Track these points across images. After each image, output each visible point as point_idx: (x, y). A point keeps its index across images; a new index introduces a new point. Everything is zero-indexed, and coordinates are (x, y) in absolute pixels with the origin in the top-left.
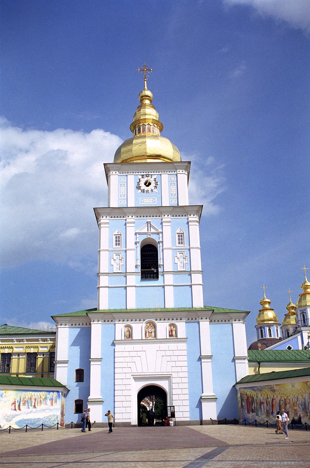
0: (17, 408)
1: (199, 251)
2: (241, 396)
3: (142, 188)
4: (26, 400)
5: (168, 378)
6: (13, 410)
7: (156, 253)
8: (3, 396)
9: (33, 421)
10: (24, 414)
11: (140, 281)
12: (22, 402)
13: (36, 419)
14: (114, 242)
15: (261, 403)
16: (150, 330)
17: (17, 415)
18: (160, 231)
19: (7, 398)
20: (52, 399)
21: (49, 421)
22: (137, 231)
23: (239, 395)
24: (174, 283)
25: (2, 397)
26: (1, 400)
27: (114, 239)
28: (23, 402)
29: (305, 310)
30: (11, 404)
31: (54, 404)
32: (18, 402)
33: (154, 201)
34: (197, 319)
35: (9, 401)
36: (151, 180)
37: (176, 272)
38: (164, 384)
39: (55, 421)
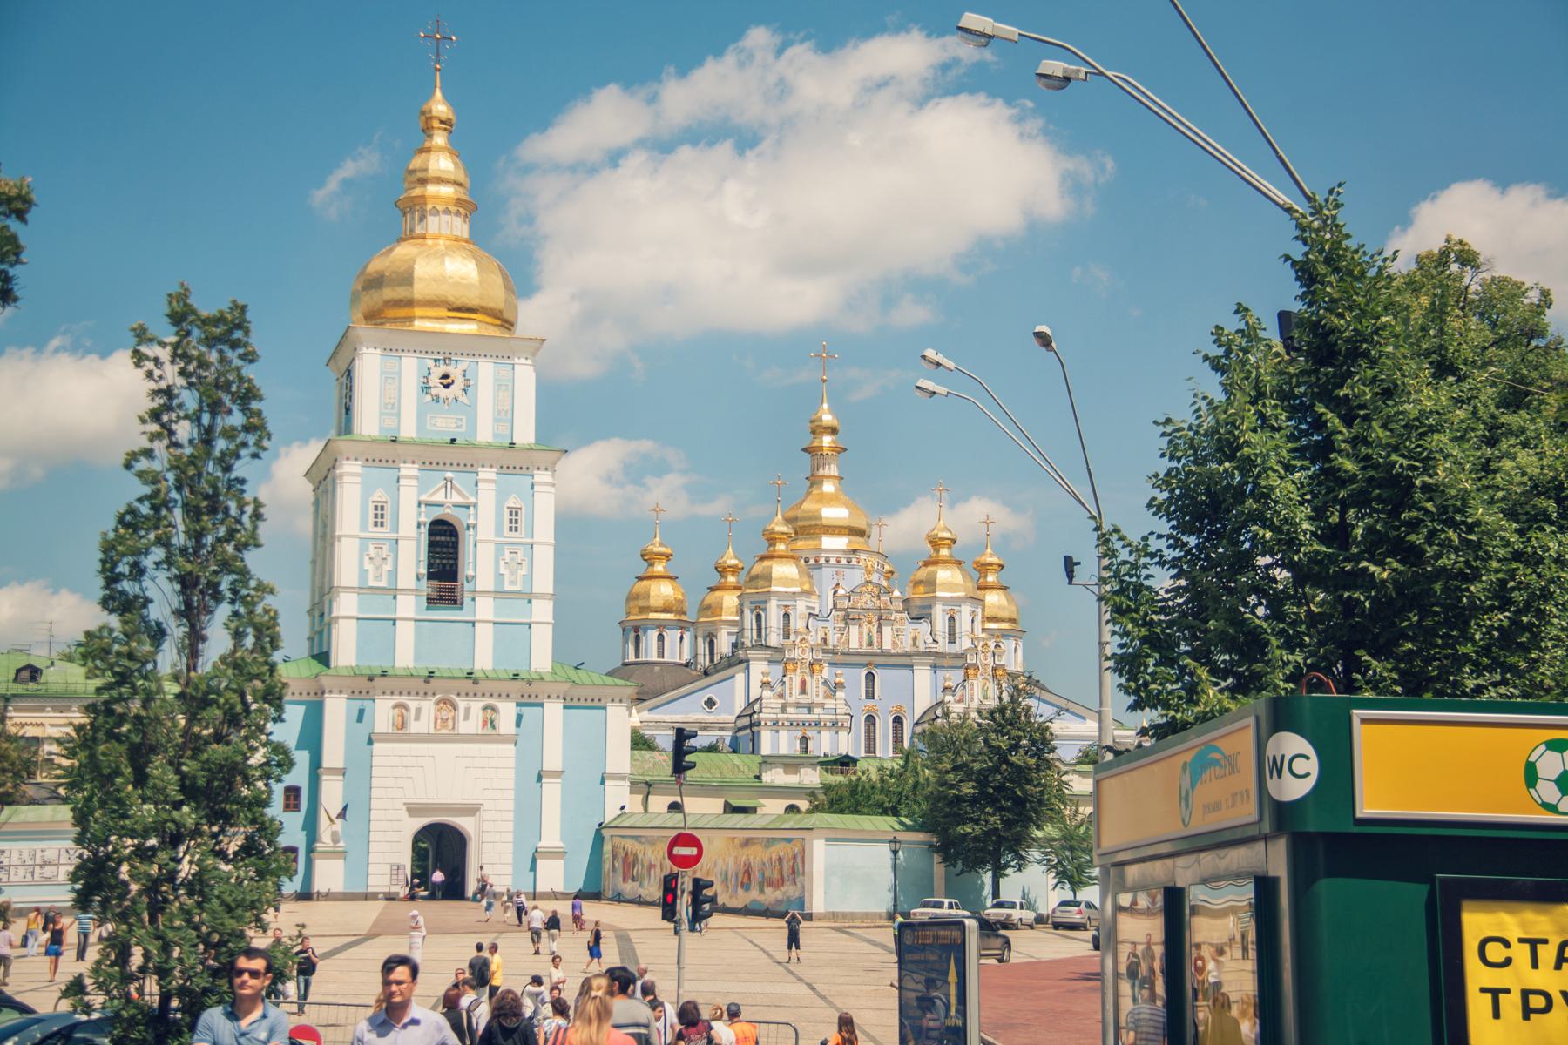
1: (552, 549)
2: (613, 851)
3: (434, 391)
5: (472, 811)
7: (453, 539)
11: (428, 609)
14: (371, 520)
15: (651, 866)
16: (444, 715)
18: (472, 500)
22: (424, 498)
23: (607, 848)
24: (496, 614)
27: (371, 512)
29: (765, 602)
33: (459, 423)
34: (540, 697)
36: (455, 372)
37: (499, 594)
38: (464, 823)
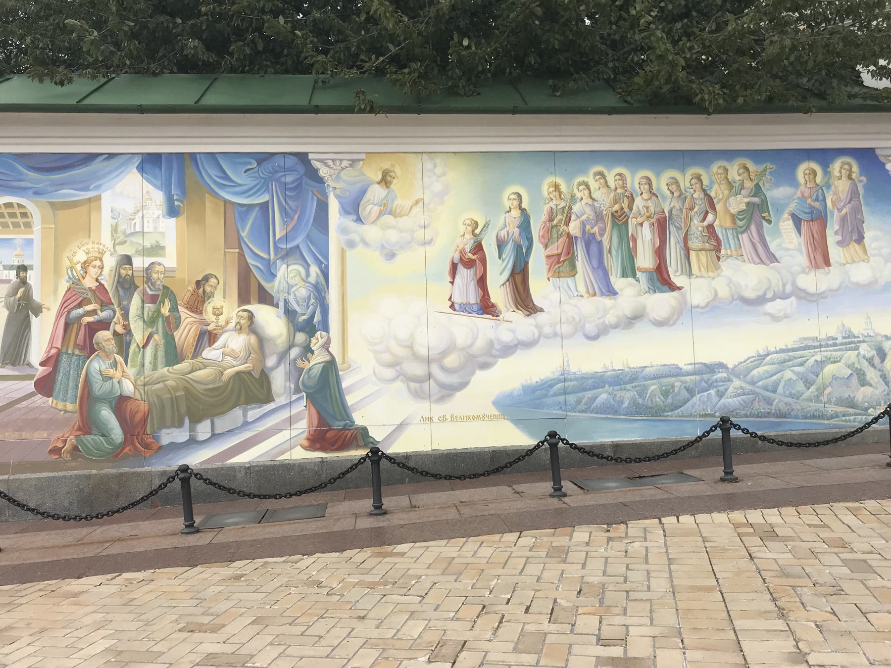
0: (499, 294)
4: (574, 228)
6: (465, 308)
8: (363, 213)
9: (653, 387)
10: (571, 335)
12: (537, 246)
13: (677, 372)
17: (508, 350)
19: (403, 222)
20: (819, 218)
21: (808, 384)
25: (359, 220)
26: (355, 237)
28: (554, 249)
30: (448, 267)
31: (835, 252)
32: (509, 249)
35: (425, 243)
39: (864, 382)
